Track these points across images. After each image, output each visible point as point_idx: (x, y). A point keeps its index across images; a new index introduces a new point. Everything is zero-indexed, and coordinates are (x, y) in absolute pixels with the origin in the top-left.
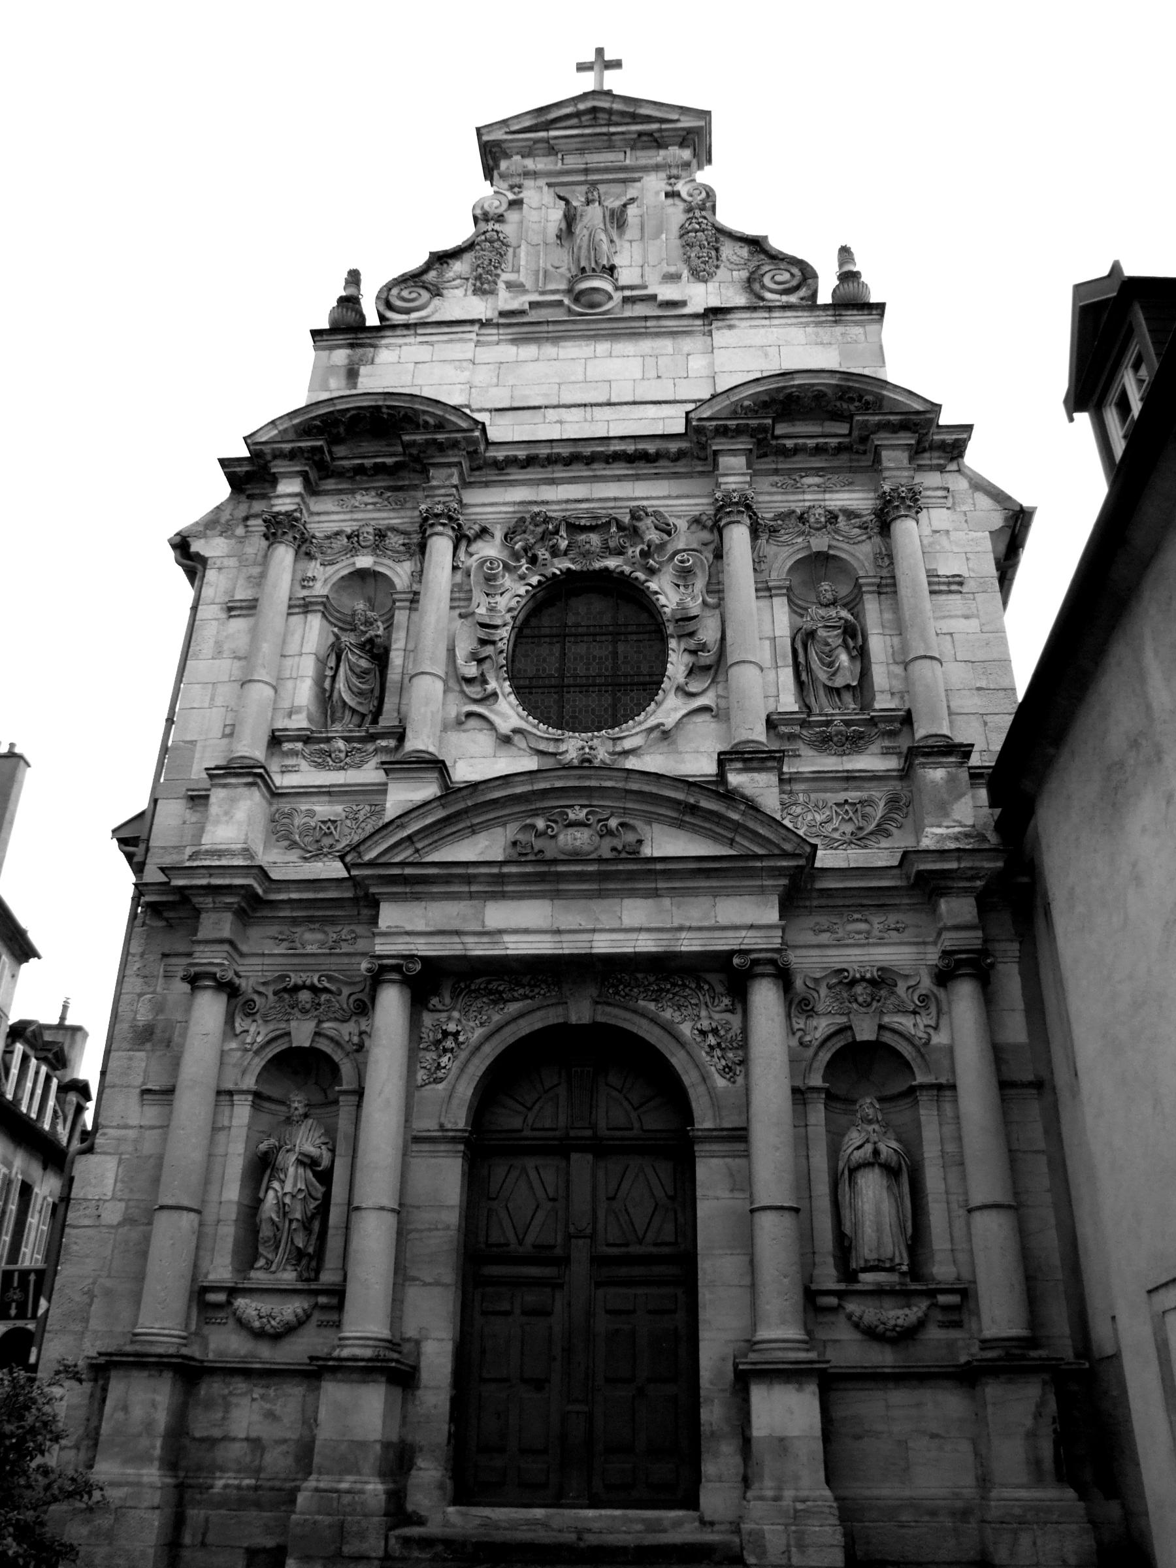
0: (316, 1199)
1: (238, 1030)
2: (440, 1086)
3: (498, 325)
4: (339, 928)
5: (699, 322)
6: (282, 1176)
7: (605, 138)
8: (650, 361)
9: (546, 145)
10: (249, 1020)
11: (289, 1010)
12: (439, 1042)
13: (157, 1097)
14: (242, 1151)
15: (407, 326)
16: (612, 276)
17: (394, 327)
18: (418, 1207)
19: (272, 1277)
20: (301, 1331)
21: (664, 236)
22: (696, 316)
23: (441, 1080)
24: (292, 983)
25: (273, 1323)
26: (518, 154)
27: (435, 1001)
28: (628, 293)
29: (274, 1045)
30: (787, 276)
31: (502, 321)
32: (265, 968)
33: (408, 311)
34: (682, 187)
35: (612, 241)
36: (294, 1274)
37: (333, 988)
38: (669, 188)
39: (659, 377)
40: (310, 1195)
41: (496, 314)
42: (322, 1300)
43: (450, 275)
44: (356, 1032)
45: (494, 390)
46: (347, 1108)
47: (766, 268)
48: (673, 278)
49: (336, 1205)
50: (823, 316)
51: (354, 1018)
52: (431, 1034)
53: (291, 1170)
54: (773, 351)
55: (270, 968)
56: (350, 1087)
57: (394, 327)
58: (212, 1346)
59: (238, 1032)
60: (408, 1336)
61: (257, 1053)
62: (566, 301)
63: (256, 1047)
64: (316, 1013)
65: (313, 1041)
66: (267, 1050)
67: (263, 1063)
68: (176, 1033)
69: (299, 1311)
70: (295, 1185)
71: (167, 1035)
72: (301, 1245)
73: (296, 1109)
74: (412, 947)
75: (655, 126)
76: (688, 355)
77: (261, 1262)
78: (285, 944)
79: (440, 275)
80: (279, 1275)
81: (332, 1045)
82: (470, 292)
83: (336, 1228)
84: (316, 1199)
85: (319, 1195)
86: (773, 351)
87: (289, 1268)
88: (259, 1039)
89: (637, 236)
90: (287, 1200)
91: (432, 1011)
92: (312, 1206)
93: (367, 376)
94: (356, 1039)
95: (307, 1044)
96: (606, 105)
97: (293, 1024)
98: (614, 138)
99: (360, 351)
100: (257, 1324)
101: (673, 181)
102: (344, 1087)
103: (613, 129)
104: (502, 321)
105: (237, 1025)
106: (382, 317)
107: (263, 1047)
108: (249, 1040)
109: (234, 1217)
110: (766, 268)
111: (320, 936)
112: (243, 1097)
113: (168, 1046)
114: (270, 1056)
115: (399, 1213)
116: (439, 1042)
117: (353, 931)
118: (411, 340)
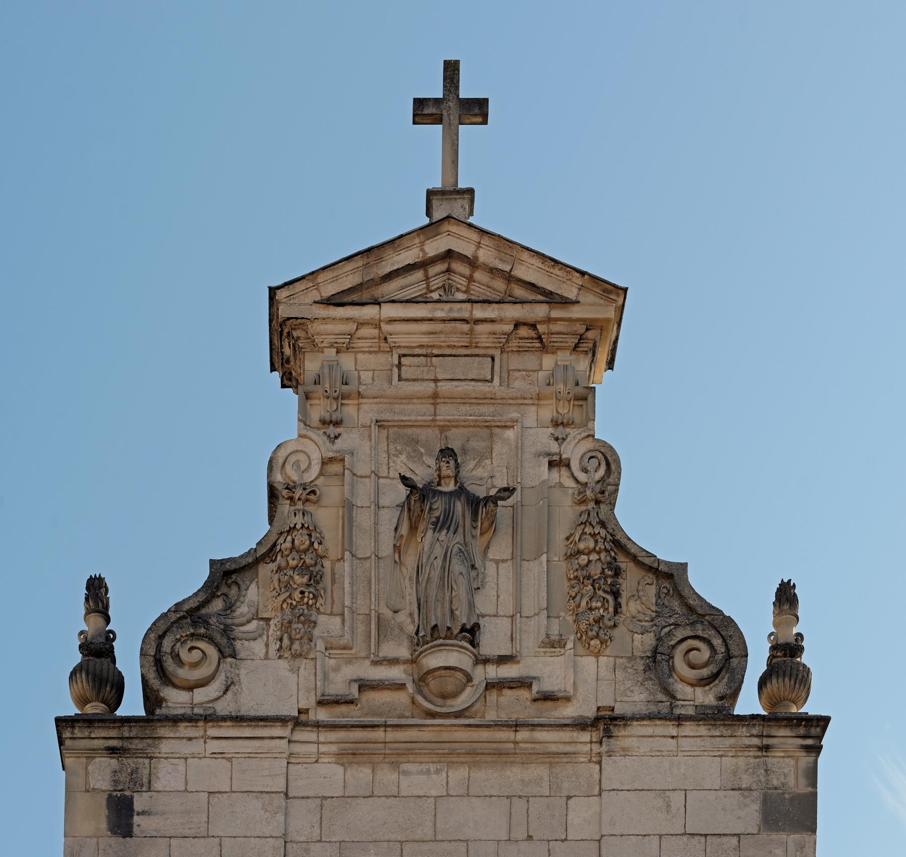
3: (318, 726)
5: (585, 736)
7: (466, 327)
8: (520, 805)
9: (375, 332)
15: (192, 719)
16: (473, 643)
17: (175, 720)
21: (544, 558)
22: (581, 725)
26: (331, 346)
28: (493, 672)
30: (705, 654)
31: (322, 715)
33: (190, 688)
34: (574, 451)
35: (473, 567)
38: (554, 447)
39: (530, 838)
41: (312, 701)
43: (243, 610)
45: (316, 848)
47: (680, 634)
48: (554, 644)
50: (745, 736)
54: (677, 799)
57: (175, 720)
62: (410, 688)
75: (541, 311)
76: (569, 798)
79: (230, 607)
82: (274, 647)
86: (677, 799)
89: (507, 555)
93: (143, 813)
96: (467, 250)
98: (479, 328)
99: (131, 762)
101: (560, 432)
103: (479, 312)
104: (322, 715)
106: (151, 699)
110: (680, 634)
118: (197, 747)
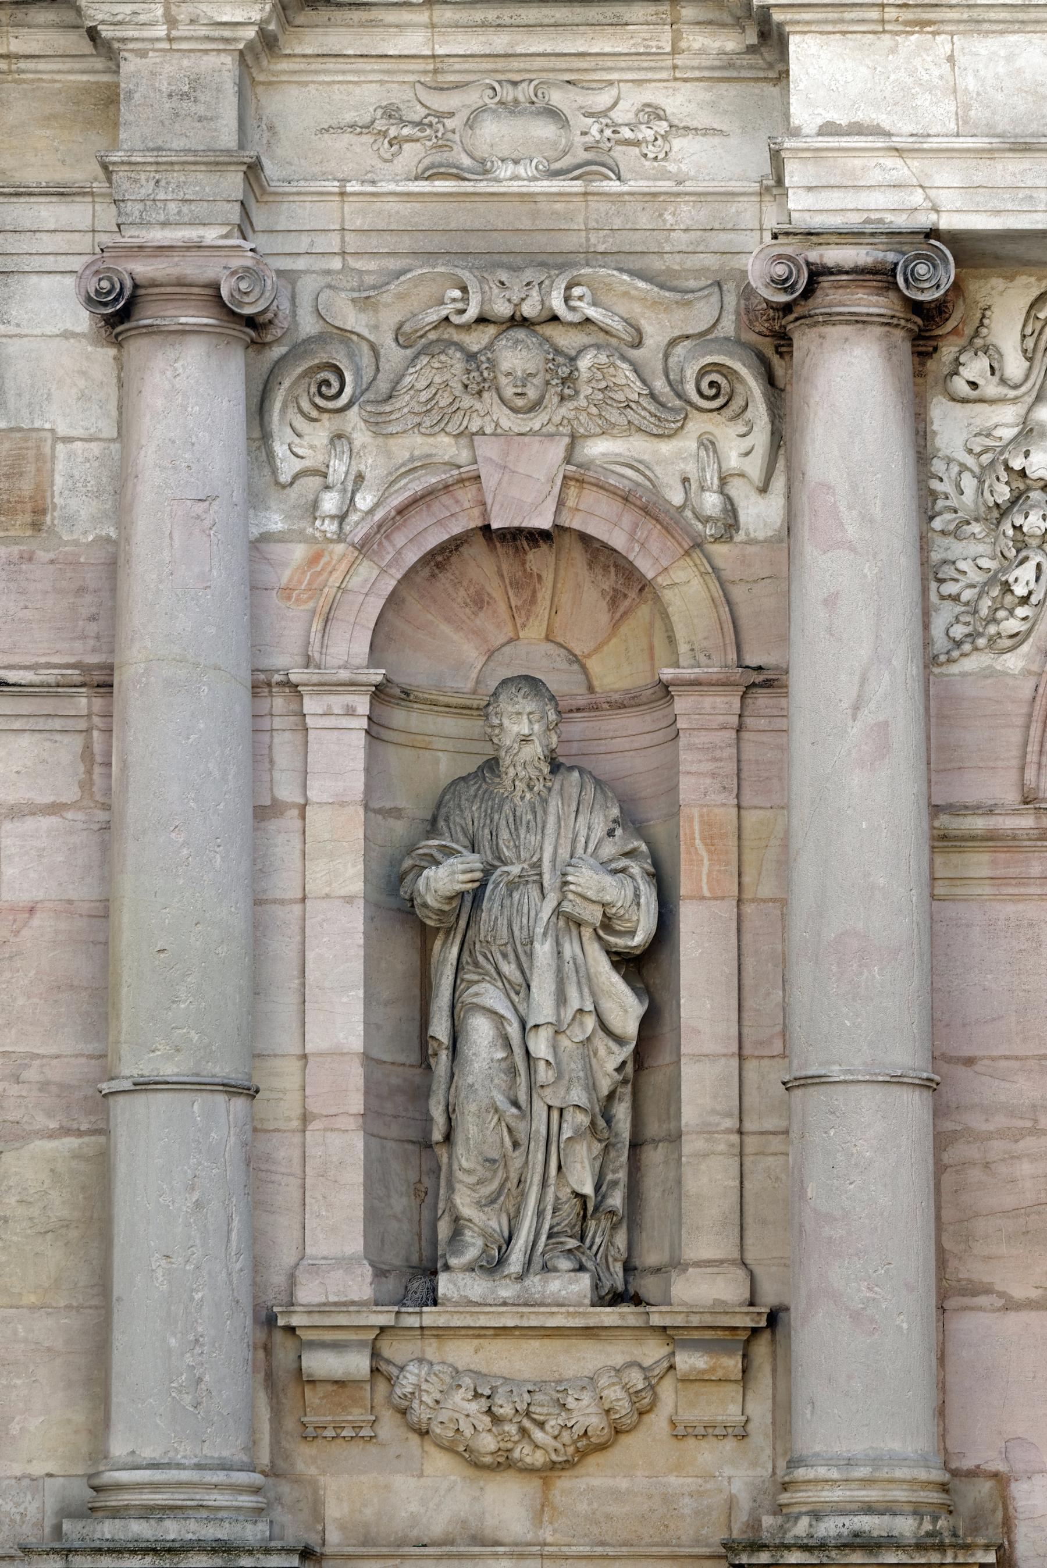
0: (620, 1040)
1: (288, 467)
2: (1014, 662)
4: (602, 99)
6: (509, 969)
10: (318, 435)
11: (467, 401)
12: (1003, 511)
13: (25, 706)
14: (358, 887)
18: (970, 1061)
19: (507, 1291)
20: (616, 1454)
23: (1017, 638)
24: (472, 312)
25: (538, 1435)
27: (975, 368)
29: (419, 521)
32: (353, 243)
36: (585, 1281)
37: (616, 325)
40: (603, 1026)
42: (688, 1361)
44: (712, 478)
46: (702, 739)
49: (700, 1057)
51: (697, 425)
52: (969, 483)
53: (543, 950)
55: (373, 243)
56: (713, 670)
58: (334, 1510)
59: (284, 478)
60: (967, 1464)
61: (364, 548)
63: (358, 529)
64: (565, 410)
65: (561, 503)
66: (400, 539)
67: (389, 584)
68: (59, 480)
69: (615, 1394)
70: (561, 999)
71: (26, 487)
72: (588, 1189)
73: (526, 740)
74: (917, 198)
77: (473, 1248)
78: (412, 155)
80: (534, 1282)
81: (628, 519)
83: (707, 1131)
84: (620, 1040)
85: (630, 1028)
87: (565, 1264)
88: (364, 501)
90: (540, 1046)
91: (965, 401)
92: (611, 1064)
94: (711, 502)
95: (544, 523)
97: (487, 448)
100: (488, 1443)
102: (688, 673)
105: (280, 449)
107: (385, 529)
108: (330, 503)
109: (356, 1103)
111: (545, 130)
112: (337, 702)
113: (36, 526)
114: (412, 557)
115: (929, 1085)
116: (1003, 511)
117: (656, 113)
